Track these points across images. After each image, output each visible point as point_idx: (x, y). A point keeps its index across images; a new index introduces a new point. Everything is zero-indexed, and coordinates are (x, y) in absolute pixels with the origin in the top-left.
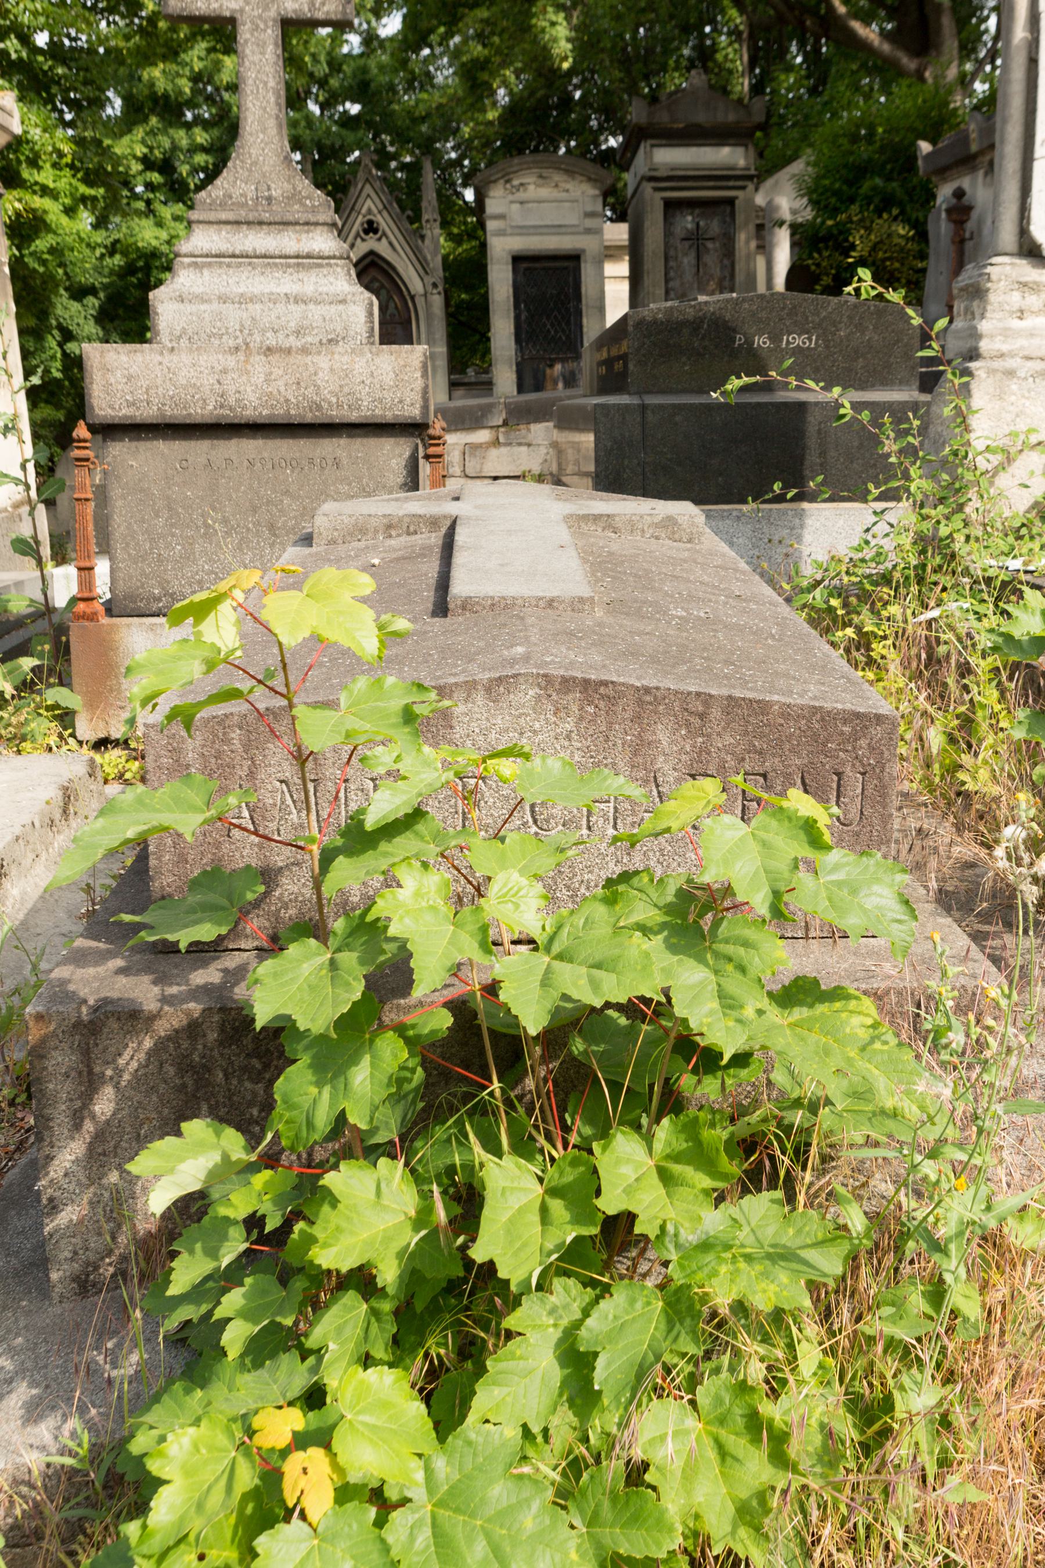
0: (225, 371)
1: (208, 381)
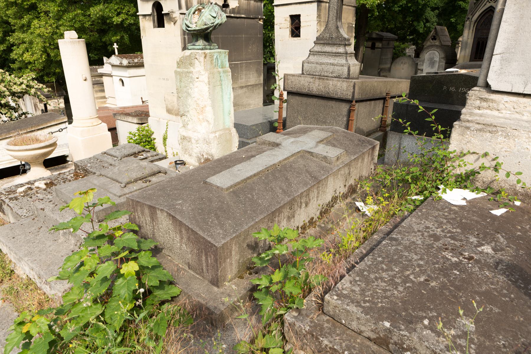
0: (310, 82)
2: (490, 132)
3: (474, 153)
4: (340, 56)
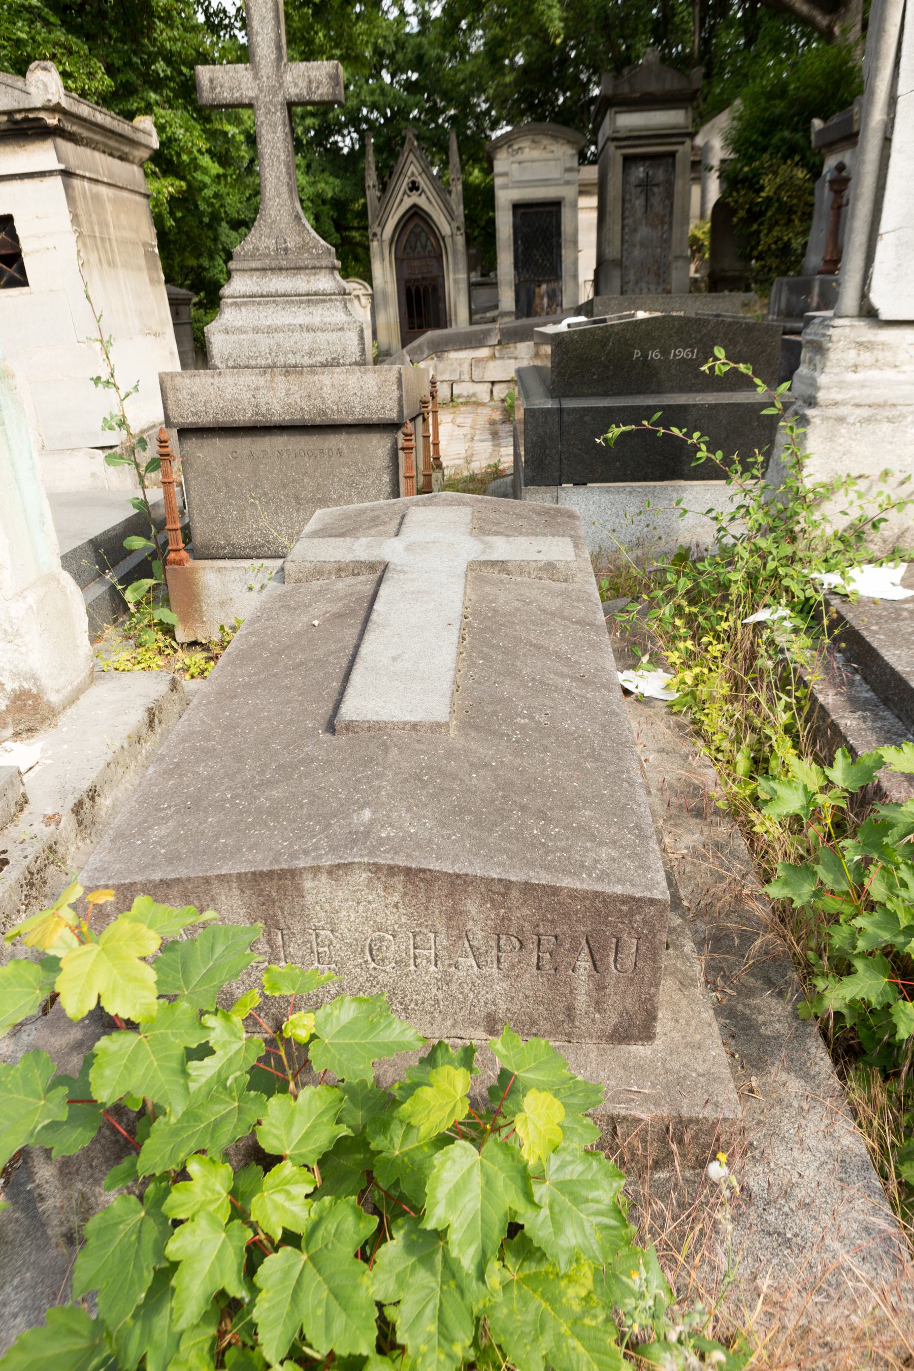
0: (257, 389)
1: (246, 396)
2: (889, 420)
3: (860, 477)
4: (324, 301)
